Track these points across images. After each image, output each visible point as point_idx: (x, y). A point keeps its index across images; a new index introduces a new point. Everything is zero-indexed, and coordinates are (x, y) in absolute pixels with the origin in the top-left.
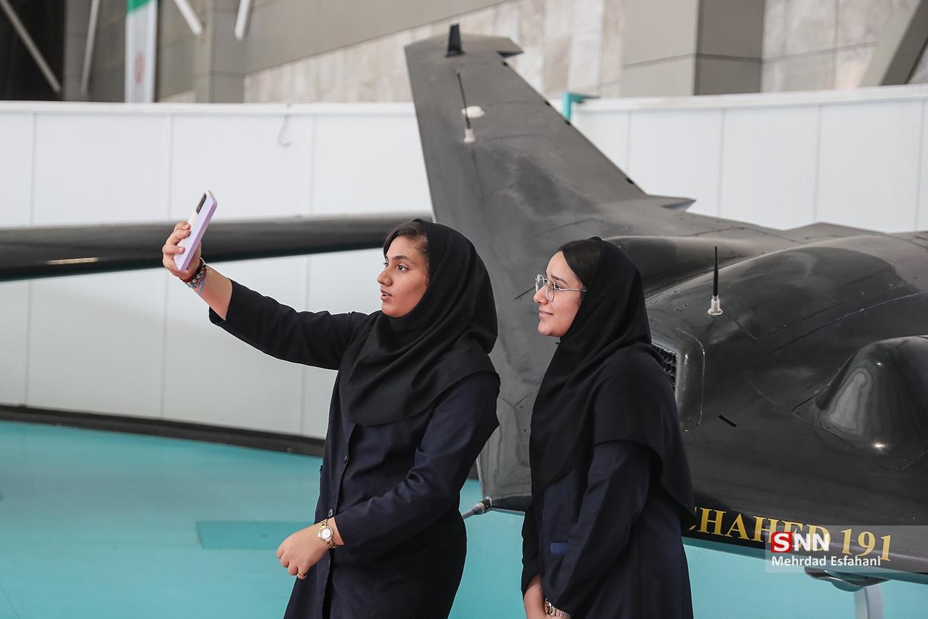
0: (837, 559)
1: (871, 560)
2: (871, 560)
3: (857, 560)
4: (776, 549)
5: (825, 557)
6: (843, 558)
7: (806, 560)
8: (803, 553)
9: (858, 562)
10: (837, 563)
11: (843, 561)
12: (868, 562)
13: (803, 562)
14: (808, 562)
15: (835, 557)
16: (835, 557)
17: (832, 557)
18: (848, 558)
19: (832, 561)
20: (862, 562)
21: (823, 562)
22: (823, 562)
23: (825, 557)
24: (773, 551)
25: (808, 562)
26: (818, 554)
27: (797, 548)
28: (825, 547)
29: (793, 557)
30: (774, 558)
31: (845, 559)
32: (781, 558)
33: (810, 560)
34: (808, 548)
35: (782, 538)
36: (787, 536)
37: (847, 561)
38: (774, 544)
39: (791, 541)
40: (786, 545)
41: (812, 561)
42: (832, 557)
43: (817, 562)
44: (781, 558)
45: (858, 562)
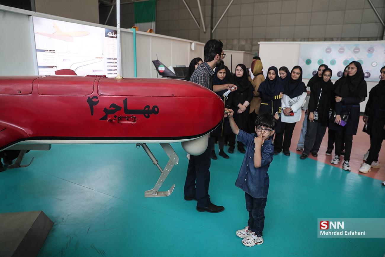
0: (347, 232)
1: (362, 233)
2: (362, 233)
3: (355, 233)
4: (322, 228)
5: (342, 231)
6: (350, 232)
7: (335, 232)
8: (333, 230)
9: (356, 233)
10: (347, 234)
11: (350, 233)
12: (360, 233)
13: (333, 233)
14: (335, 233)
15: (347, 231)
16: (347, 231)
17: (345, 231)
18: (352, 232)
19: (345, 233)
20: (358, 233)
21: (341, 233)
22: (341, 233)
23: (342, 231)
24: (321, 229)
25: (335, 233)
26: (340, 230)
27: (330, 228)
28: (343, 227)
29: (329, 231)
30: (321, 232)
31: (351, 232)
32: (324, 232)
33: (336, 233)
34: (335, 227)
35: (324, 223)
36: (326, 222)
37: (352, 233)
38: (321, 226)
39: (328, 224)
40: (326, 226)
41: (337, 233)
42: (345, 231)
43: (339, 233)
44: (324, 232)
45: (356, 233)
